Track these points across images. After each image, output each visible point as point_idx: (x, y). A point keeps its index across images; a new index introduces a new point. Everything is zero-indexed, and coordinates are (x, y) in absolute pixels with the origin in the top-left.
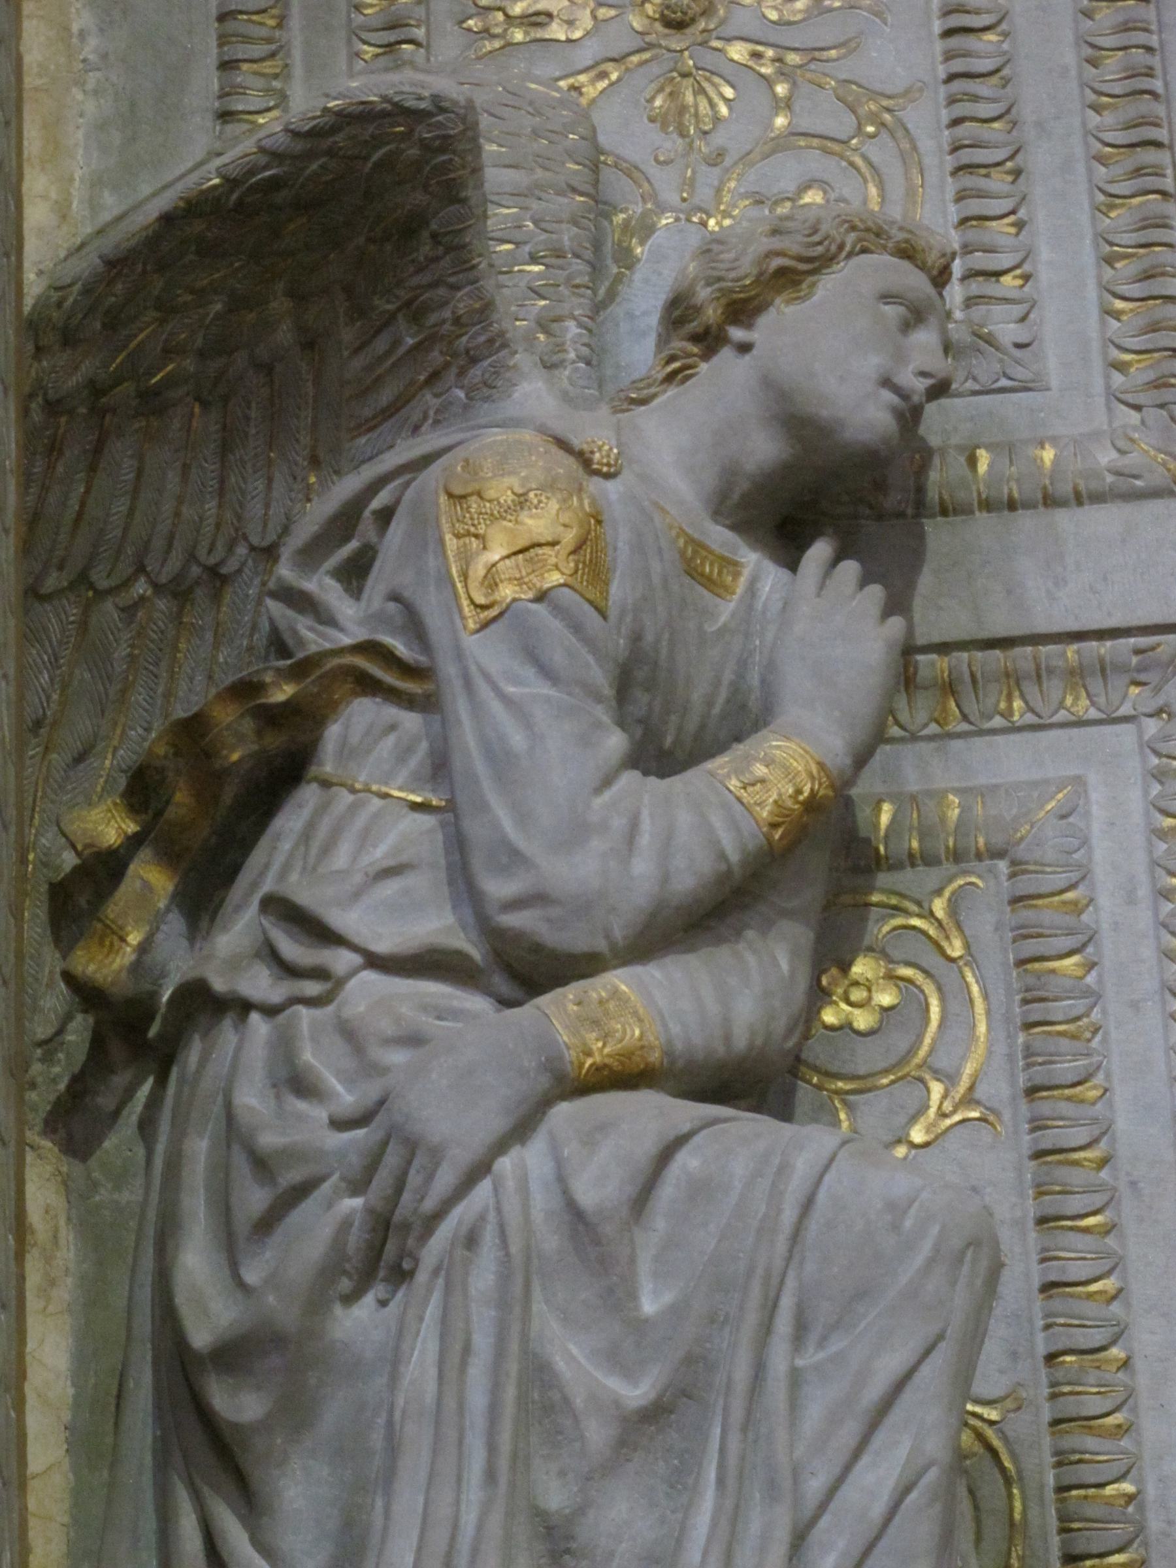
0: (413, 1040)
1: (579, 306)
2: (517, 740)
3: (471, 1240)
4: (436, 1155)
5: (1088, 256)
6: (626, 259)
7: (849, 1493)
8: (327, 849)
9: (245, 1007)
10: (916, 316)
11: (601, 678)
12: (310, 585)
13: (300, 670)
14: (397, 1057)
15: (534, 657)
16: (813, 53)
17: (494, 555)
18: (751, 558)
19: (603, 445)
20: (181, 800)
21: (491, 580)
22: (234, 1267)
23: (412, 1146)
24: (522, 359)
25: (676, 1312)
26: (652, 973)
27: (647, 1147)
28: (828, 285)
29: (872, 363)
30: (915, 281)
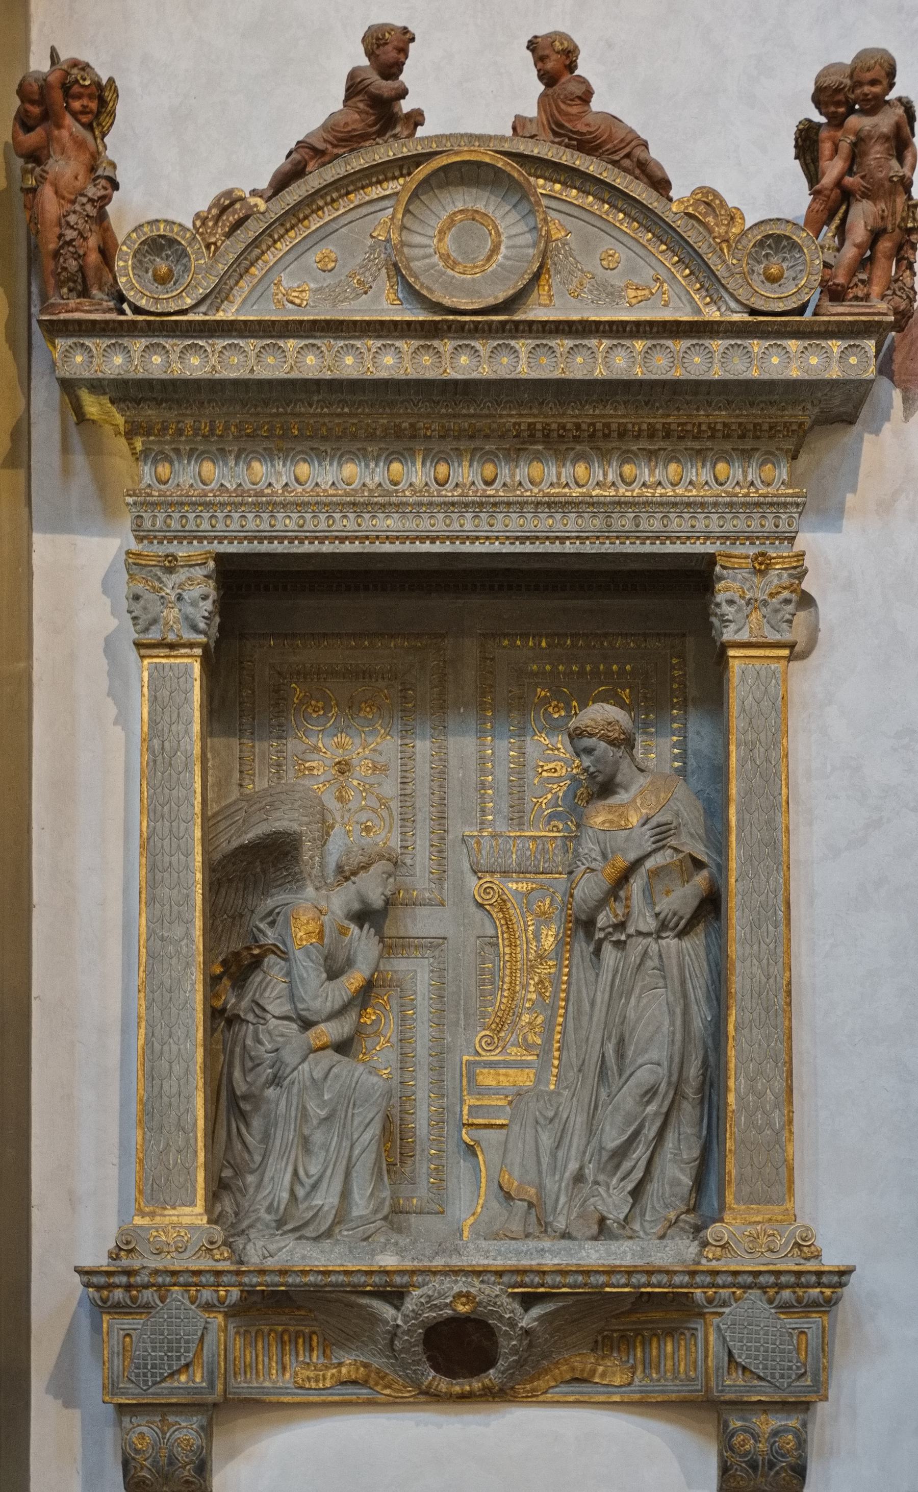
0: (282, 1035)
1: (318, 852)
2: (305, 975)
3: (293, 1083)
4: (287, 1065)
5: (428, 844)
6: (328, 834)
7: (361, 1139)
8: (265, 990)
9: (248, 1022)
10: (390, 876)
11: (322, 961)
12: (261, 926)
13: (260, 947)
14: (280, 1039)
15: (309, 957)
16: (371, 785)
17: (301, 934)
18: (352, 926)
19: (323, 905)
20: (233, 969)
21: (301, 940)
22: (245, 1077)
23: (282, 1063)
24: (308, 882)
25: (331, 1099)
26: (328, 1024)
27: (327, 1068)
28: (372, 869)
29: (380, 890)
30: (389, 866)
